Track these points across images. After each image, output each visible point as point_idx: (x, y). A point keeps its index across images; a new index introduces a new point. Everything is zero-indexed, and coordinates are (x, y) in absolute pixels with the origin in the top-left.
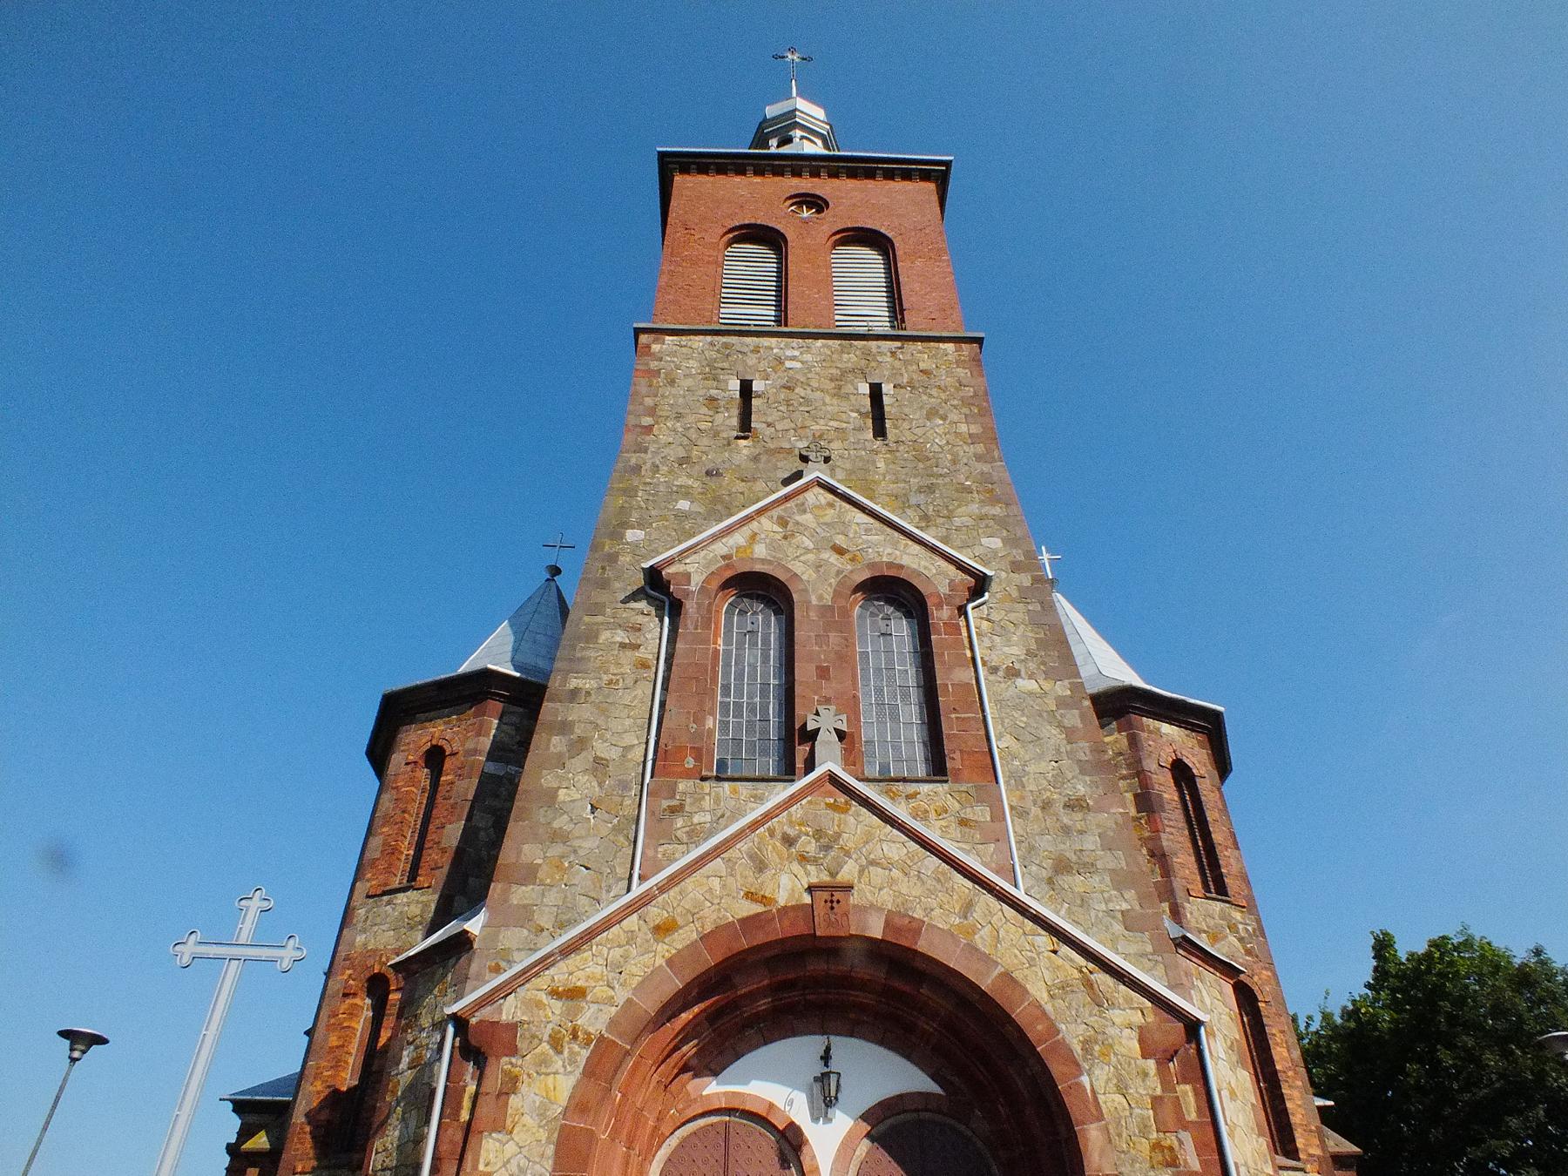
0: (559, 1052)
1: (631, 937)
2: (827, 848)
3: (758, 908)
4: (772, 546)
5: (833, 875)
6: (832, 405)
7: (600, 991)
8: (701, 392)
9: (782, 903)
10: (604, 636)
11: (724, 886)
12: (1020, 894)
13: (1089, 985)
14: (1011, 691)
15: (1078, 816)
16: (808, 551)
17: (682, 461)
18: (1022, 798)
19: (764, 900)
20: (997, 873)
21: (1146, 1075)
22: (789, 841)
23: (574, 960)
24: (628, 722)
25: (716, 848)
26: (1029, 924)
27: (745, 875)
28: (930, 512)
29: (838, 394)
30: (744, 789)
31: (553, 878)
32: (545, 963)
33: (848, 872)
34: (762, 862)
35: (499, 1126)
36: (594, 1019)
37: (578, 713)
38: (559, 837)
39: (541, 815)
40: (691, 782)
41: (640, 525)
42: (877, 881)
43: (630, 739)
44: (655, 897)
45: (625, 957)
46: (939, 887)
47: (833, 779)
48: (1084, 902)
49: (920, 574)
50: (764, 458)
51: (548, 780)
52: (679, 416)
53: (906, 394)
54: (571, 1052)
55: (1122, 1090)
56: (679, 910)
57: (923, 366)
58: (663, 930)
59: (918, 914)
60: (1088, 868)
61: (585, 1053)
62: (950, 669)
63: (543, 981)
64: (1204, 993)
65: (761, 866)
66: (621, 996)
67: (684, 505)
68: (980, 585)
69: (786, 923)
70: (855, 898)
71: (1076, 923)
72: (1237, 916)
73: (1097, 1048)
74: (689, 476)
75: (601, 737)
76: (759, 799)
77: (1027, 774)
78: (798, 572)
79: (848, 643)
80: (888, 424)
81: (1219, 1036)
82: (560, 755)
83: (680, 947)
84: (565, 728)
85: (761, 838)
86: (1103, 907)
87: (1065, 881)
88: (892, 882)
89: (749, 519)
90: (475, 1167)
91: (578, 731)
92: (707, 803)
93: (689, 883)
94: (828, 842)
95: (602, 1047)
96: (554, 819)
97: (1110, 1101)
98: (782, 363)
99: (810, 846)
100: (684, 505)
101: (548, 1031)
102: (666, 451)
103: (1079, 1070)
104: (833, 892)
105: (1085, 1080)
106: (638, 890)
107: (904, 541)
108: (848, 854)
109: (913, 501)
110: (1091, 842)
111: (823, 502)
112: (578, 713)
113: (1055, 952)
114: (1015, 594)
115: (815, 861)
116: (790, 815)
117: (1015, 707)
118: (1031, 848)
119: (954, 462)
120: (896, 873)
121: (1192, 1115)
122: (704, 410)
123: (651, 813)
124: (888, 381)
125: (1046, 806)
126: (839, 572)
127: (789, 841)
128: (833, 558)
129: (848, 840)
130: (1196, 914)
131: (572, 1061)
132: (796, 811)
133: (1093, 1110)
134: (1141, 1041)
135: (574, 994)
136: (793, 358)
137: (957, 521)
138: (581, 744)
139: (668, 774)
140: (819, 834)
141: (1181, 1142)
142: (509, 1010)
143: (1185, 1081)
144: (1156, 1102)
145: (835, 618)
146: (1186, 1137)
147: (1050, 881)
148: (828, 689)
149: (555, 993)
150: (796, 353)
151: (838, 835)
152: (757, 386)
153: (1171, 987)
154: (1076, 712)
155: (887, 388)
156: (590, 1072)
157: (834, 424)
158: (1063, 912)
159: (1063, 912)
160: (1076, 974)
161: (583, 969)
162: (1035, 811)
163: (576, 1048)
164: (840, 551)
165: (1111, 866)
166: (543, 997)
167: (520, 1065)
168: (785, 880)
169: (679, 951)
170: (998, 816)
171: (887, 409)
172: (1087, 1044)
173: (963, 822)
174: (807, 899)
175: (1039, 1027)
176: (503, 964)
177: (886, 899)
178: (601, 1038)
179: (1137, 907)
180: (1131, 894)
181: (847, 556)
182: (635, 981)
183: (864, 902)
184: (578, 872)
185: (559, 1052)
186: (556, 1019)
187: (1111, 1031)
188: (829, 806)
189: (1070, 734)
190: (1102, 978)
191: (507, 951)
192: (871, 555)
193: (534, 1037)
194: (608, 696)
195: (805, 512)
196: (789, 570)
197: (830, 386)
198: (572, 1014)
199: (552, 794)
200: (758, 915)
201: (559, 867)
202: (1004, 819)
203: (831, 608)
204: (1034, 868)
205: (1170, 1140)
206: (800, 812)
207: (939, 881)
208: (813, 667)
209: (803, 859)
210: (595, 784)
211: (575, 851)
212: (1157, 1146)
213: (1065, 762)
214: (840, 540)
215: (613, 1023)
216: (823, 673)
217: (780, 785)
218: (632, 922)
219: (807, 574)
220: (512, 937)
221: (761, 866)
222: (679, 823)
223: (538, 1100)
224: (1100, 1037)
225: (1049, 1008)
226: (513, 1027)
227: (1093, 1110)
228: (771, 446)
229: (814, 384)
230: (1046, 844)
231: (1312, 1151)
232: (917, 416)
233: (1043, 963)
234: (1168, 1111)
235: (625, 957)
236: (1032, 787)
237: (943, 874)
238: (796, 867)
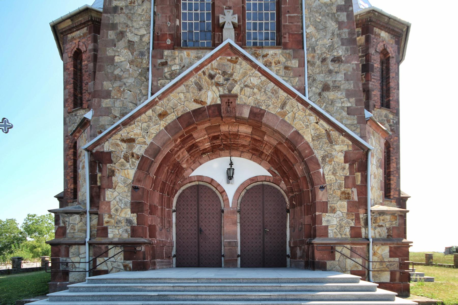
1: (150, 118)
2: (227, 80)
3: (198, 106)
5: (230, 91)
11: (185, 97)
15: (337, 65)
18: (313, 57)
19: (202, 102)
20: (298, 90)
21: (344, 169)
22: (211, 77)
23: (128, 128)
24: (141, 23)
25: (181, 80)
26: (308, 112)
30: (193, 53)
31: (117, 96)
34: (200, 86)
38: (118, 78)
39: (109, 69)
40: (170, 51)
42: (248, 94)
43: (143, 32)
44: (157, 102)
45: (149, 126)
46: (273, 96)
48: (333, 102)
51: (110, 52)
54: (132, 162)
55: (334, 174)
56: (168, 107)
58: (162, 115)
59: (263, 108)
60: (337, 88)
61: (138, 162)
64: (373, 141)
65: (200, 88)
66: (149, 141)
69: (210, 111)
70: (238, 101)
71: (328, 112)
73: (327, 159)
75: (130, 31)
76: (199, 58)
81: (375, 157)
82: (113, 40)
83: (169, 122)
84: (114, 27)
86: (340, 105)
87: (325, 94)
88: (254, 94)
90: (104, 200)
91: (120, 28)
92: (177, 61)
93: (171, 96)
94: (227, 76)
95: (143, 159)
96: (115, 70)
97: (329, 177)
99: (220, 79)
101: (123, 154)
103: (319, 166)
104: (229, 98)
105: (321, 170)
106: (150, 99)
108: (236, 82)
110: (340, 77)
113: (317, 123)
115: (222, 85)
116: (212, 65)
118: (314, 80)
120: (256, 90)
121: (359, 183)
123: (154, 66)
125: (324, 60)
127: (211, 77)
129: (236, 76)
132: (215, 63)
133: (322, 180)
135: (131, 141)
138: (122, 34)
140: (224, 73)
144: (346, 178)
146: (355, 190)
147: (320, 94)
149: (123, 141)
151: (232, 75)
153: (361, 137)
156: (140, 168)
158: (323, 107)
159: (323, 107)
160: (324, 132)
161: (134, 131)
162: (318, 63)
163: (134, 160)
165: (347, 87)
167: (116, 166)
168: (210, 94)
169: (169, 124)
170: (302, 65)
172: (324, 158)
173: (286, 68)
174: (219, 102)
176: (102, 130)
177: (251, 101)
179: (354, 105)
180: (353, 100)
183: (242, 103)
186: (125, 150)
190: (335, 134)
193: (117, 156)
194: (130, 10)
198: (131, 148)
199: (112, 59)
200: (199, 109)
202: (304, 66)
204: (314, 89)
205: (349, 190)
206: (216, 64)
209: (218, 85)
210: (130, 53)
211: (125, 84)
213: (336, 39)
215: (146, 151)
217: (208, 51)
218: (150, 112)
220: (104, 120)
221: (200, 88)
222: (166, 70)
223: (123, 178)
224: (329, 155)
225: (311, 145)
227: (322, 180)
230: (320, 78)
233: (311, 127)
234: (350, 182)
235: (149, 126)
237: (275, 90)
238: (214, 88)
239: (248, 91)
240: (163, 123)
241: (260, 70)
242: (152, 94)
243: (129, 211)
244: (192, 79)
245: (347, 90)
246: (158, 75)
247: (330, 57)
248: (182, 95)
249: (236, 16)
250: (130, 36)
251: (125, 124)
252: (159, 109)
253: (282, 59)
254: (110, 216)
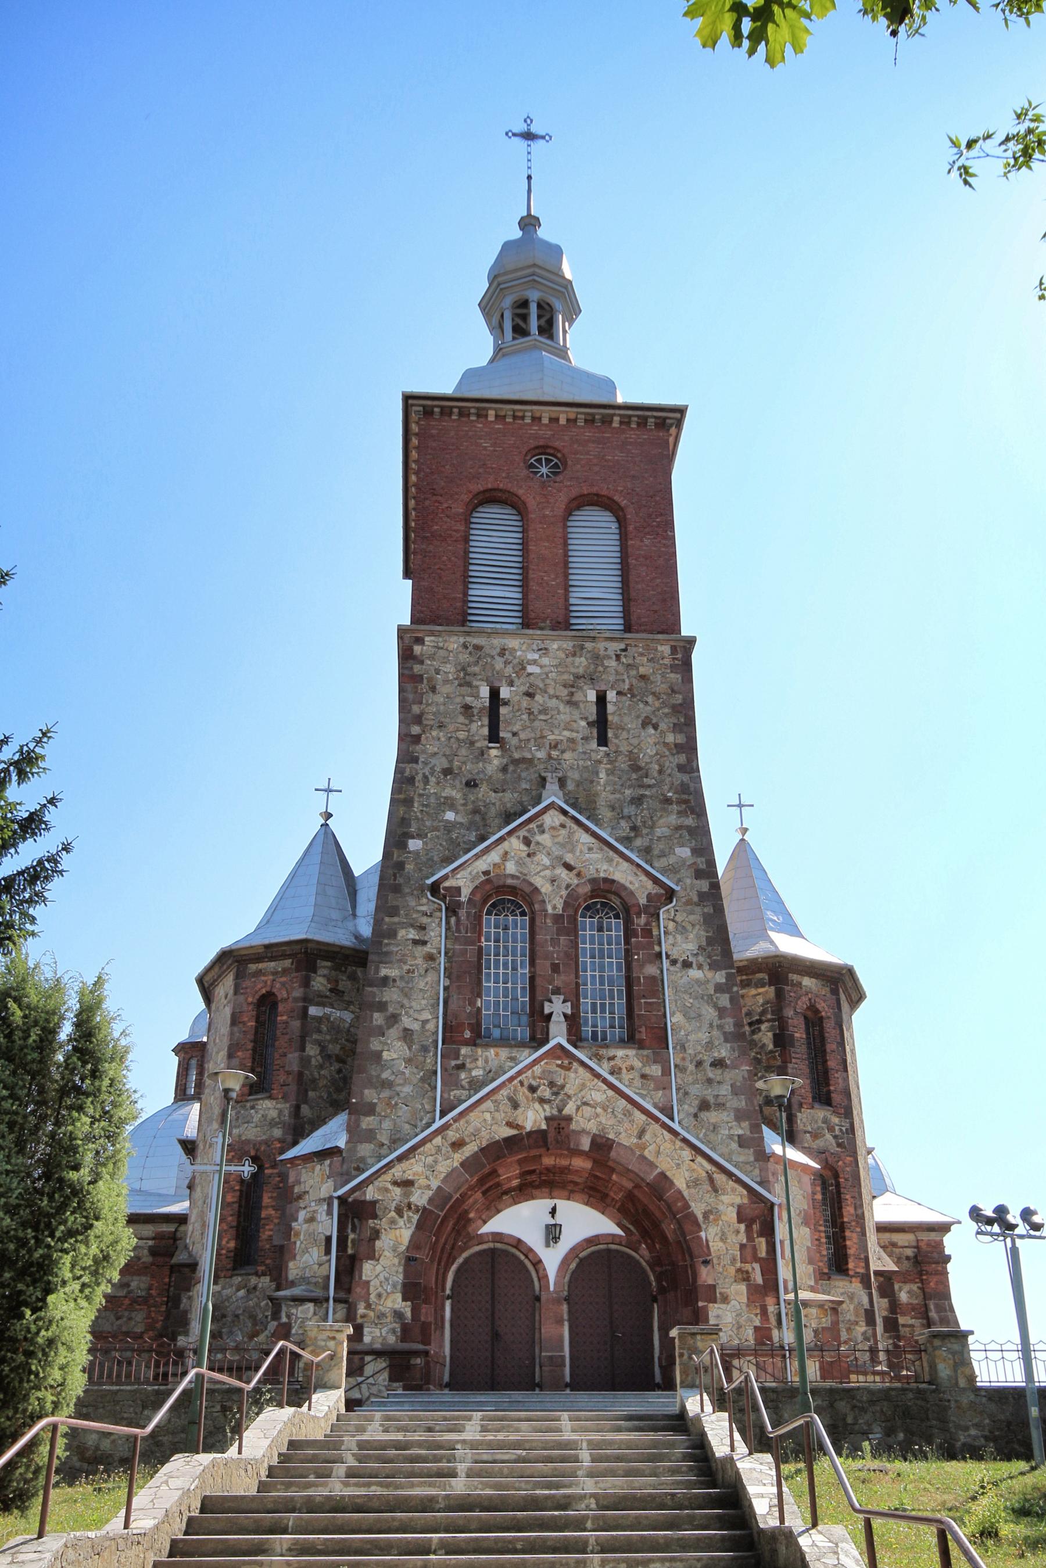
0: (402, 1217)
1: (439, 1149)
2: (556, 1094)
3: (514, 1132)
4: (520, 863)
5: (560, 1111)
6: (565, 713)
7: (423, 1182)
8: (458, 700)
9: (528, 1129)
10: (402, 933)
11: (493, 1118)
12: (676, 1126)
13: (711, 1180)
14: (685, 979)
15: (719, 1071)
16: (547, 868)
17: (447, 772)
18: (684, 1059)
19: (518, 1127)
21: (738, 1232)
22: (533, 1089)
23: (405, 1165)
24: (424, 1002)
25: (488, 1094)
28: (639, 824)
29: (571, 703)
32: (389, 1166)
33: (569, 1109)
36: (420, 1198)
37: (390, 995)
38: (387, 1084)
41: (420, 836)
44: (451, 1125)
45: (436, 1162)
49: (626, 888)
50: (511, 768)
51: (375, 1045)
52: (441, 726)
53: (626, 700)
54: (409, 1217)
55: (723, 1239)
56: (466, 1133)
57: (642, 670)
58: (457, 1145)
59: (611, 1136)
60: (720, 1106)
61: (416, 1217)
62: (642, 967)
63: (388, 1177)
65: (515, 1106)
66: (435, 1184)
67: (450, 816)
68: (670, 895)
72: (836, 1120)
74: (453, 787)
75: (407, 1013)
77: (688, 1041)
78: (538, 886)
80: (610, 734)
82: (380, 1027)
84: (382, 1007)
85: (515, 1087)
86: (727, 1132)
87: (704, 1115)
89: (502, 839)
92: (480, 1063)
97: (716, 1246)
98: (524, 668)
99: (545, 1092)
100: (450, 816)
101: (394, 1204)
102: (433, 761)
103: (700, 1229)
105: (703, 1234)
107: (617, 858)
108: (569, 1097)
109: (626, 811)
110: (725, 1090)
111: (557, 823)
112: (390, 995)
113: (693, 1161)
114: (695, 899)
115: (549, 1101)
116: (533, 1072)
117: (685, 992)
118: (686, 1093)
119: (660, 772)
120: (599, 1110)
122: (461, 719)
123: (444, 1069)
124: (612, 688)
125: (699, 1064)
126: (568, 886)
127: (533, 1089)
128: (562, 873)
129: (569, 1089)
130: (804, 1120)
131: (409, 1220)
132: (537, 1069)
134: (738, 1213)
136: (534, 662)
137: (658, 832)
138: (394, 1019)
139: (454, 1042)
140: (552, 1084)
141: (753, 1269)
143: (761, 1235)
144: (742, 1246)
145: (567, 924)
147: (696, 1116)
148: (559, 981)
149: (395, 1183)
150: (536, 656)
151: (563, 1087)
152: (505, 693)
154: (727, 996)
155: (611, 696)
157: (566, 733)
162: (691, 1067)
163: (411, 1214)
164: (569, 867)
166: (390, 1187)
171: (610, 718)
172: (706, 1215)
173: (644, 1076)
174: (544, 1127)
175: (679, 1204)
177: (592, 1127)
178: (425, 1209)
179: (748, 1133)
180: (746, 1124)
181: (575, 872)
182: (443, 1175)
183: (578, 1129)
184: (401, 1108)
185: (402, 1217)
186: (398, 1198)
187: (721, 1207)
188: (558, 1066)
189: (722, 1012)
191: (362, 1159)
192: (591, 872)
193: (386, 1208)
195: (543, 832)
196: (531, 884)
197: (564, 692)
198: (407, 1195)
199: (378, 1055)
201: (388, 1104)
203: (562, 916)
205: (748, 1267)
207: (625, 1115)
208: (548, 963)
209: (542, 1101)
210: (406, 1048)
212: (739, 1270)
213: (715, 1033)
214: (569, 858)
215: (431, 1200)
216: (555, 968)
218: (438, 1140)
219: (545, 888)
221: (515, 1106)
222: (463, 1076)
223: (392, 1243)
225: (686, 1194)
226: (374, 1203)
228: (517, 756)
229: (551, 691)
230: (695, 1090)
231: (858, 1270)
232: (632, 724)
235: (436, 1162)
236: (690, 1051)
238: (537, 1105)
249: (569, 1004)
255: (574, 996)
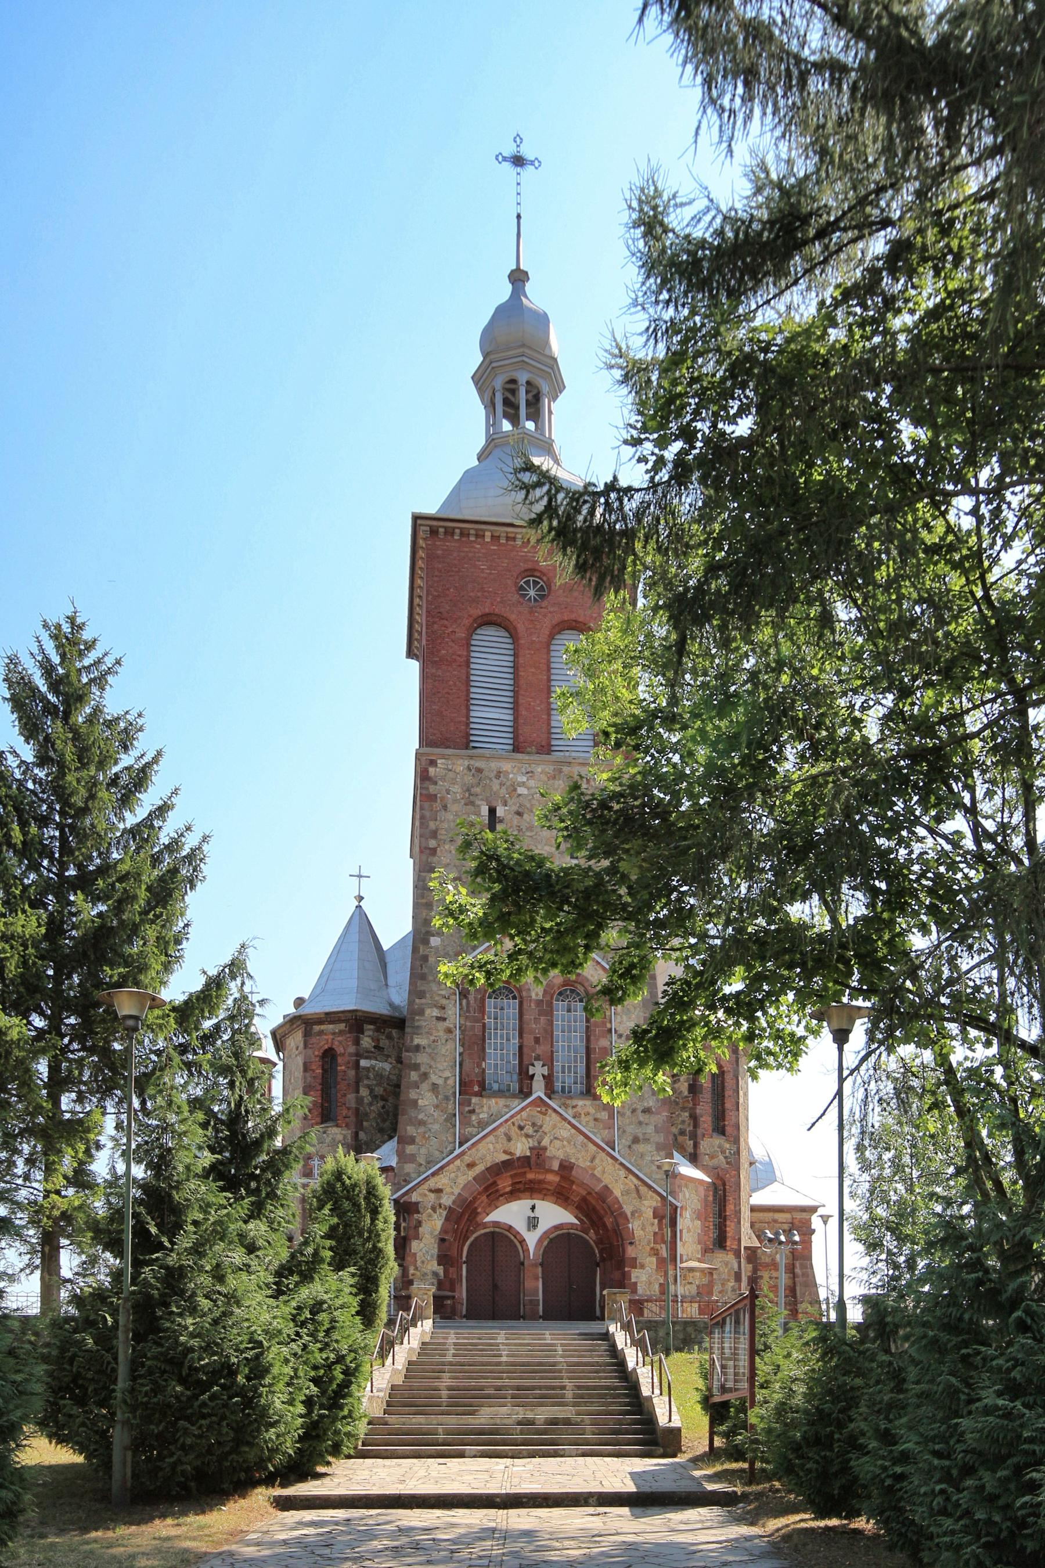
1: (459, 1169)
3: (508, 1157)
12: (616, 1154)
13: (638, 1191)
19: (511, 1154)
22: (521, 1128)
27: (502, 1143)
32: (426, 1179)
33: (545, 1142)
35: (417, 1237)
36: (447, 1200)
37: (421, 1058)
38: (422, 1123)
39: (412, 1113)
43: (447, 1074)
47: (540, 1098)
58: (471, 1166)
63: (426, 1186)
65: (509, 1139)
66: (457, 1191)
70: (548, 1154)
79: (551, 1023)
84: (416, 1067)
87: (635, 1147)
92: (485, 1109)
93: (480, 1146)
95: (450, 1210)
99: (529, 1130)
110: (650, 1129)
112: (421, 1058)
125: (634, 1111)
127: (521, 1128)
135: (439, 1191)
138: (425, 1076)
139: (467, 1094)
140: (534, 1125)
142: (415, 1197)
148: (540, 1050)
149: (431, 1191)
162: (628, 1113)
168: (519, 1145)
173: (596, 1120)
177: (560, 1154)
198: (439, 1198)
199: (416, 1102)
209: (527, 1136)
215: (454, 1202)
216: (537, 1040)
218: (458, 1162)
221: (509, 1139)
226: (417, 1204)
230: (631, 1129)
234: (659, 1237)
238: (524, 1139)
239: (557, 1143)
240: (472, 1174)
241: (570, 1123)
242: (461, 1144)
243: (435, 1263)
244: (502, 1130)
245: (658, 1144)
246: (465, 1122)
247: (640, 1108)
248: (491, 1146)
250: (434, 1078)
251: (433, 1174)
252: (467, 1159)
253: (592, 1111)
254: (416, 1269)
255: (549, 1062)
